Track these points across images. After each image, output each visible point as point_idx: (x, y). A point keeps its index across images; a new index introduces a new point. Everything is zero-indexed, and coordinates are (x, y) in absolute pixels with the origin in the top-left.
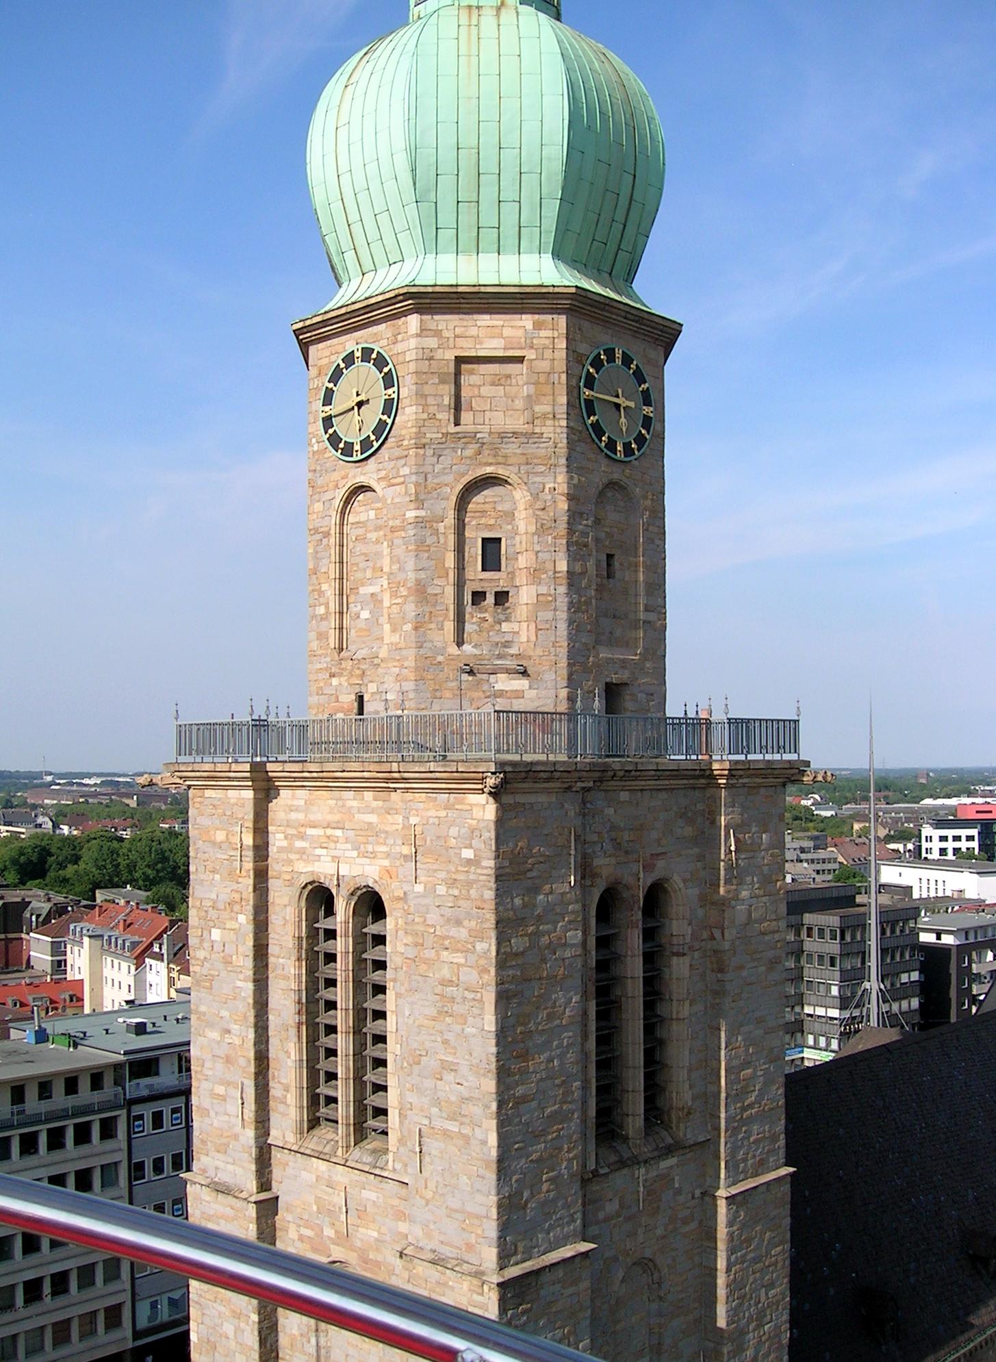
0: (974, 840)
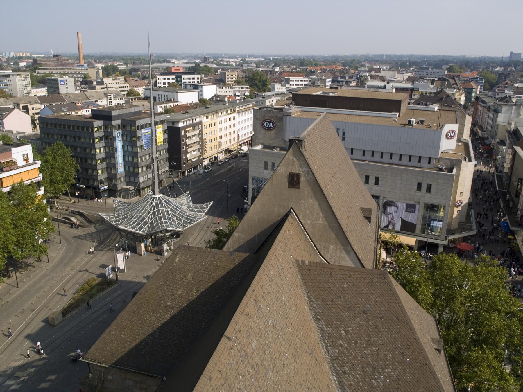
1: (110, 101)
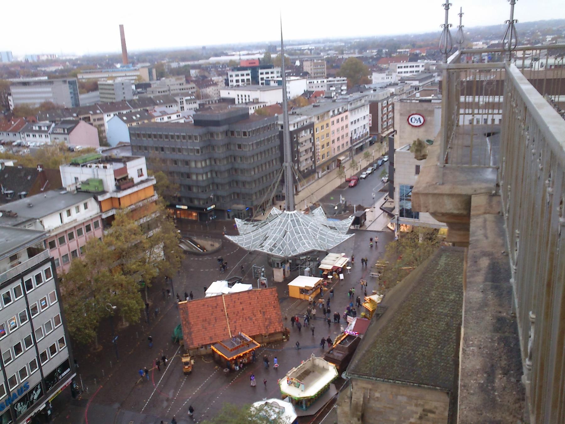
1: (182, 106)
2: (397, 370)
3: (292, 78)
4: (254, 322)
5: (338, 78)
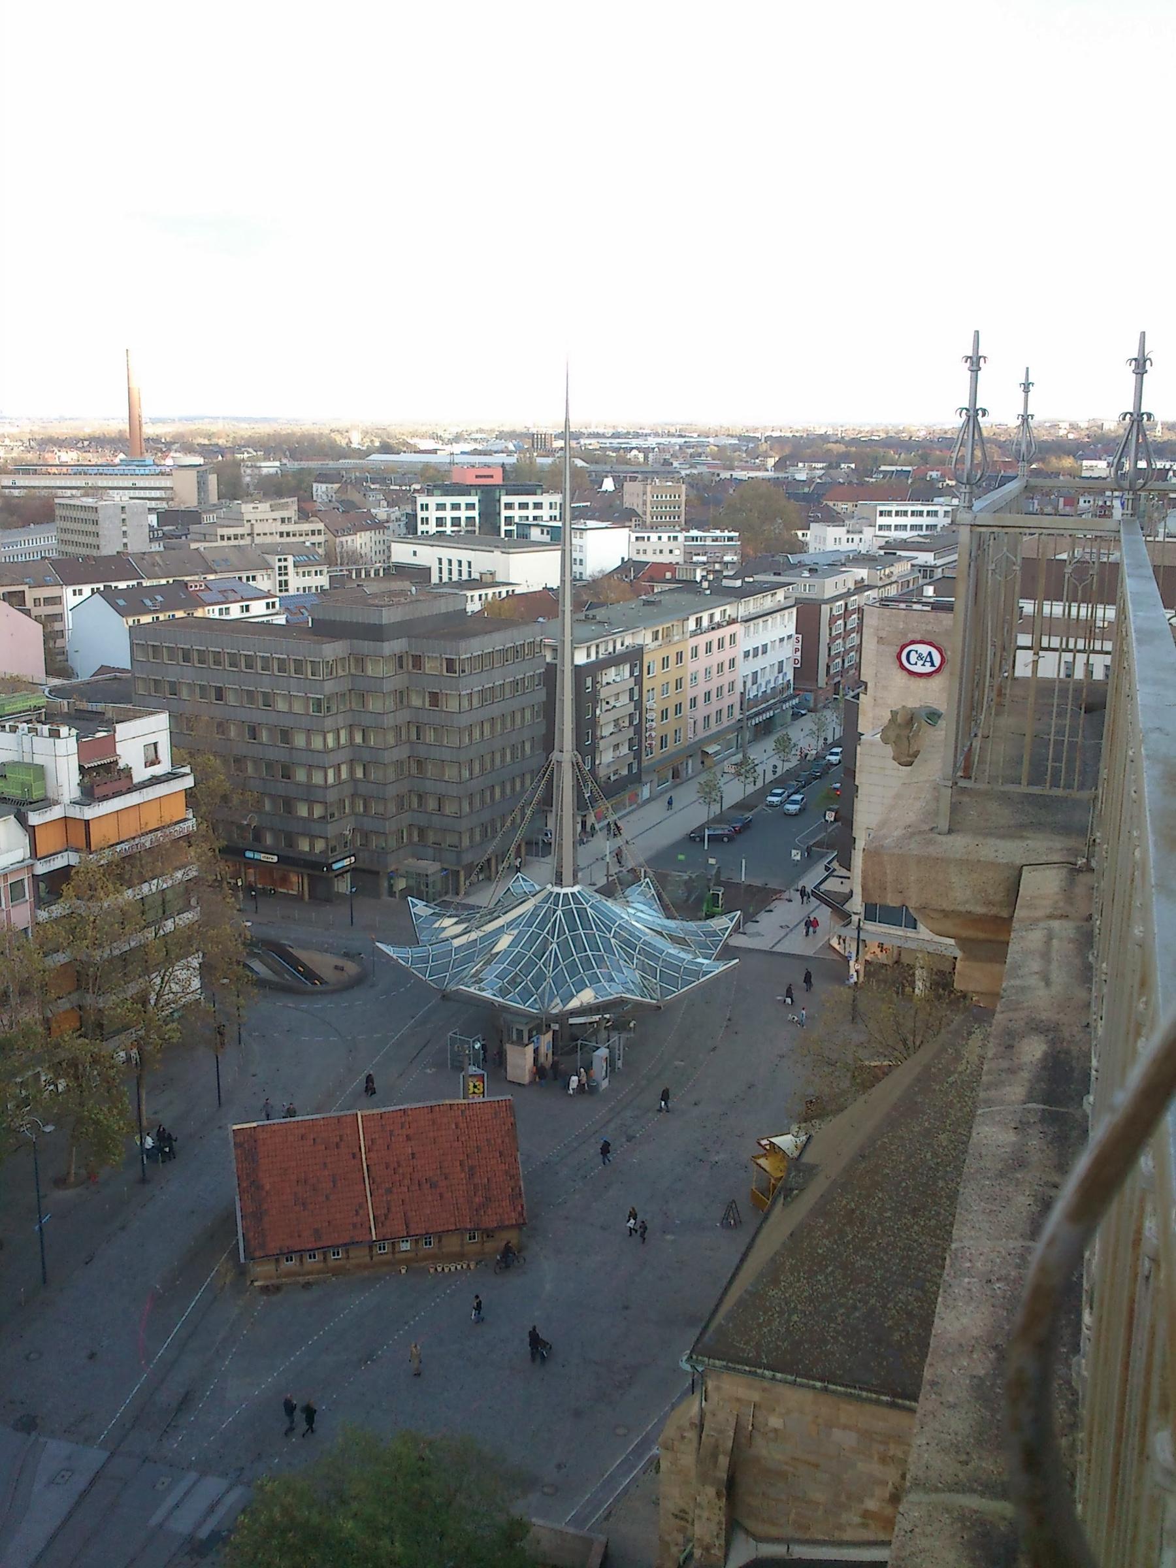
0: (474, 509)
1: (283, 578)
2: (833, 1354)
3: (591, 524)
4: (441, 1195)
5: (718, 533)
